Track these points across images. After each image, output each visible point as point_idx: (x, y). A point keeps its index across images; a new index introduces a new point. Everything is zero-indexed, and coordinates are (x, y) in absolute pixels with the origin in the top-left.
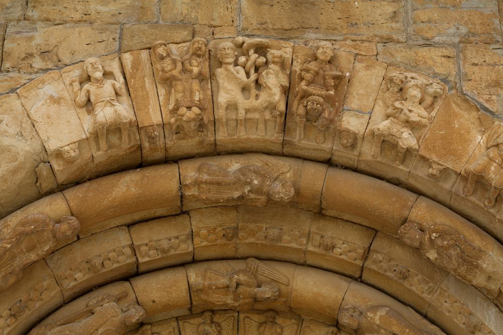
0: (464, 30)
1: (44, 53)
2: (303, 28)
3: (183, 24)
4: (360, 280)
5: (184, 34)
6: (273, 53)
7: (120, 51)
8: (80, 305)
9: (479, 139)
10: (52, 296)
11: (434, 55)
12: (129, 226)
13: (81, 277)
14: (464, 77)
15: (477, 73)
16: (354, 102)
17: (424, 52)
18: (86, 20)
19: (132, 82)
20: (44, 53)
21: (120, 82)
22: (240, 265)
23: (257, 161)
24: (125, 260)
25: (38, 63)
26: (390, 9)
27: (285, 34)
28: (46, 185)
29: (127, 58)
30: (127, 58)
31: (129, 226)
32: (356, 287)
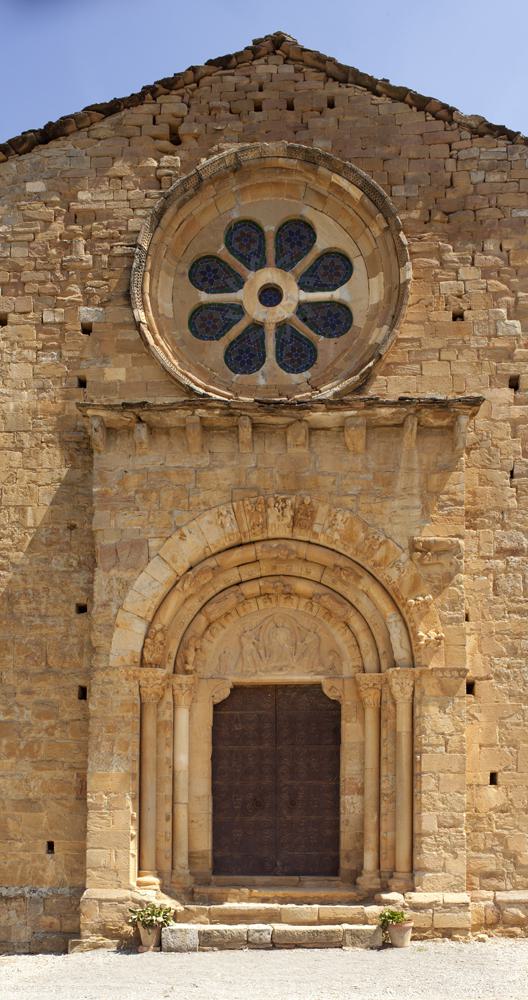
0: (360, 488)
1: (204, 503)
2: (299, 489)
3: (255, 488)
4: (320, 583)
5: (255, 494)
6: (289, 502)
7: (232, 501)
8: (222, 595)
9: (362, 535)
10: (213, 593)
11: (348, 500)
12: (238, 566)
13: (222, 586)
14: (358, 509)
15: (364, 508)
16: (317, 521)
17: (344, 499)
18: (219, 488)
19: (238, 515)
20: (204, 503)
21: (233, 516)
22: (277, 578)
23: (283, 542)
24: (237, 580)
25: (202, 507)
26: (332, 480)
27: (292, 492)
28: (208, 554)
29: (234, 504)
30: (234, 504)
31: (238, 566)
32: (318, 586)
